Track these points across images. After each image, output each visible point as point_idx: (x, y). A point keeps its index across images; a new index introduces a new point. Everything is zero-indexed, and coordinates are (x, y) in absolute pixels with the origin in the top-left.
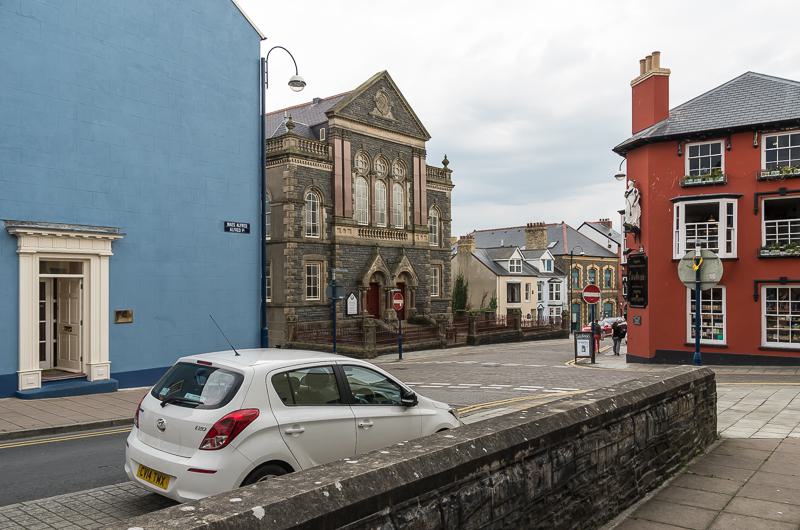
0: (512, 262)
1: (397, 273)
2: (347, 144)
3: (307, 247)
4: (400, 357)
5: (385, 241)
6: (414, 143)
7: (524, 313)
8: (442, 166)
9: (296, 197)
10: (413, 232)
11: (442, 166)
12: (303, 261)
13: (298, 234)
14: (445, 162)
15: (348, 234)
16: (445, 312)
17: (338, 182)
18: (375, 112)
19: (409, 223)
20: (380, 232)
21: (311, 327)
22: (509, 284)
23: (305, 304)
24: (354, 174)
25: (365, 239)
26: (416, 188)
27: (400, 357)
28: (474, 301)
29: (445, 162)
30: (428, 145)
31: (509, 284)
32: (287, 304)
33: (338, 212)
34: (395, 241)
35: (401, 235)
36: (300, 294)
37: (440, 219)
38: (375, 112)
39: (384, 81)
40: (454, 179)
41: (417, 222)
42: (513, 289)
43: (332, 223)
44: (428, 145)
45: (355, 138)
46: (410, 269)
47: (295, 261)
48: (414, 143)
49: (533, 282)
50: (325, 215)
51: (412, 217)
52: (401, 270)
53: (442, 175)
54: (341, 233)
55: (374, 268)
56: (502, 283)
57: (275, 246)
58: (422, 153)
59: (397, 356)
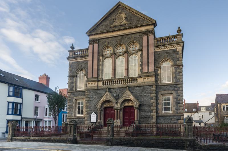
3: (76, 93)
9: (71, 75)
10: (141, 77)
15: (93, 85)
17: (90, 63)
18: (115, 24)
19: (140, 73)
20: (118, 81)
29: (179, 31)
33: (90, 76)
35: (134, 79)
38: (115, 24)
41: (145, 70)
46: (131, 97)
51: (141, 70)
52: (124, 98)
55: (104, 99)
58: (153, 32)
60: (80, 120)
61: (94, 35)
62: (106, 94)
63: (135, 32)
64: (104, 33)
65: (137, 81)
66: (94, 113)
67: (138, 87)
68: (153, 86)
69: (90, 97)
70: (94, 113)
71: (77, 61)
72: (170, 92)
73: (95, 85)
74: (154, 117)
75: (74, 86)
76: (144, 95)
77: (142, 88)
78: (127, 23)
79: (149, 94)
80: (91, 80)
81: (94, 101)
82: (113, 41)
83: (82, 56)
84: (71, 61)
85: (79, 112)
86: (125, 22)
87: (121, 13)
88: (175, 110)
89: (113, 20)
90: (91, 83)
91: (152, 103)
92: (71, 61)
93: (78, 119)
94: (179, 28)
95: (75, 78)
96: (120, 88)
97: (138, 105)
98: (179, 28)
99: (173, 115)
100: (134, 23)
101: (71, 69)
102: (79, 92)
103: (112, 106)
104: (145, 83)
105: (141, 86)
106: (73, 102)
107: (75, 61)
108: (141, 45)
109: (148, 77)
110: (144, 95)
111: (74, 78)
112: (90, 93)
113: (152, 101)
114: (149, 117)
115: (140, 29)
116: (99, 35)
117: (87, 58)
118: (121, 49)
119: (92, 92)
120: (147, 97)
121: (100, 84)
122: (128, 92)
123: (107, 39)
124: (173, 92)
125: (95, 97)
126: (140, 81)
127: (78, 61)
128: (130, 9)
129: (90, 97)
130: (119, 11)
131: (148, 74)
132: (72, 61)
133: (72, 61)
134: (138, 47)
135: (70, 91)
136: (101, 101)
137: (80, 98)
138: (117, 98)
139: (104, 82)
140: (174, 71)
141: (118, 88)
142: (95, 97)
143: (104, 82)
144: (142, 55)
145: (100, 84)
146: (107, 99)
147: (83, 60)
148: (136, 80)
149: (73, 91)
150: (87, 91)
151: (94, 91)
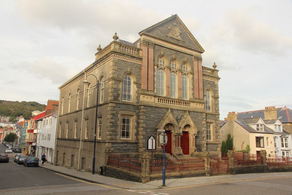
0: (258, 125)
1: (183, 126)
2: (151, 50)
4: (164, 184)
5: (176, 106)
6: (194, 53)
7: (268, 153)
8: (213, 68)
9: (116, 77)
10: (193, 102)
11: (213, 68)
12: (119, 116)
13: (116, 98)
14: (215, 66)
16: (216, 150)
17: (144, 70)
18: (170, 35)
19: (192, 97)
20: (173, 101)
21: (122, 157)
22: (257, 138)
23: (119, 141)
24: (156, 67)
25: (162, 104)
26: (196, 77)
27: (164, 184)
28: (238, 146)
29: (215, 66)
30: (203, 55)
31: (257, 138)
32: (107, 141)
33: (144, 86)
34: (183, 107)
35: (187, 103)
36: (116, 135)
37: (212, 97)
39: (174, 19)
40: (220, 74)
42: (258, 139)
43: (138, 94)
44: (203, 55)
45: (157, 47)
46: (191, 123)
47: (113, 114)
48: (194, 53)
49: (271, 137)
50: (136, 89)
51: (193, 94)
52: (185, 124)
53: (214, 72)
54: (145, 99)
55: (167, 121)
56: (252, 137)
57: (105, 106)
58: (199, 59)
59: (161, 182)
60: (129, 145)
61: (149, 36)
62: (169, 115)
63: (188, 53)
64: (161, 40)
65: (190, 105)
66: (152, 137)
67: (193, 112)
68: (204, 114)
69: (146, 115)
70: (152, 137)
71: (125, 60)
72: (212, 121)
73: (151, 101)
74: (205, 145)
75: (119, 95)
76: (198, 121)
77: (196, 113)
78: (182, 41)
79: (201, 122)
80: (147, 93)
81: (151, 122)
82: (168, 53)
83: (134, 57)
84: (116, 58)
85: (123, 133)
86: (179, 38)
87: (175, 26)
88: (215, 139)
89: (169, 29)
90: (147, 96)
91: (203, 131)
92: (116, 58)
93: (125, 144)
94: (215, 63)
95: (121, 83)
96: (178, 110)
97: (197, 132)
98: (215, 63)
99: (213, 143)
100: (187, 44)
101: (116, 68)
102: (128, 105)
103: (170, 130)
104: (198, 110)
105: (195, 112)
106: (118, 119)
107: (121, 59)
108: (193, 69)
109: (200, 104)
110: (198, 121)
111: (120, 82)
112: (147, 111)
113: (203, 129)
114: (202, 145)
115: (192, 52)
116: (154, 39)
117: (141, 61)
118: (177, 65)
119: (149, 110)
120: (200, 124)
121: (156, 99)
122: (189, 117)
123: (162, 47)
124: (214, 121)
125: (152, 116)
126: (193, 106)
127: (127, 60)
128: (184, 26)
129: (146, 115)
130: (175, 24)
131: (200, 101)
132: (118, 58)
133: (118, 58)
134: (189, 69)
135: (115, 102)
136: (164, 124)
137: (128, 114)
138: (178, 120)
139: (160, 98)
140: (214, 101)
141: (177, 110)
142: (152, 116)
143: (159, 99)
144: (193, 78)
145: (156, 99)
146: (171, 121)
147: (134, 62)
148: (189, 103)
149: (117, 102)
150: (143, 107)
151: (151, 108)
